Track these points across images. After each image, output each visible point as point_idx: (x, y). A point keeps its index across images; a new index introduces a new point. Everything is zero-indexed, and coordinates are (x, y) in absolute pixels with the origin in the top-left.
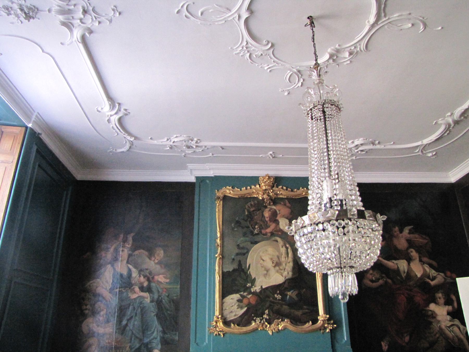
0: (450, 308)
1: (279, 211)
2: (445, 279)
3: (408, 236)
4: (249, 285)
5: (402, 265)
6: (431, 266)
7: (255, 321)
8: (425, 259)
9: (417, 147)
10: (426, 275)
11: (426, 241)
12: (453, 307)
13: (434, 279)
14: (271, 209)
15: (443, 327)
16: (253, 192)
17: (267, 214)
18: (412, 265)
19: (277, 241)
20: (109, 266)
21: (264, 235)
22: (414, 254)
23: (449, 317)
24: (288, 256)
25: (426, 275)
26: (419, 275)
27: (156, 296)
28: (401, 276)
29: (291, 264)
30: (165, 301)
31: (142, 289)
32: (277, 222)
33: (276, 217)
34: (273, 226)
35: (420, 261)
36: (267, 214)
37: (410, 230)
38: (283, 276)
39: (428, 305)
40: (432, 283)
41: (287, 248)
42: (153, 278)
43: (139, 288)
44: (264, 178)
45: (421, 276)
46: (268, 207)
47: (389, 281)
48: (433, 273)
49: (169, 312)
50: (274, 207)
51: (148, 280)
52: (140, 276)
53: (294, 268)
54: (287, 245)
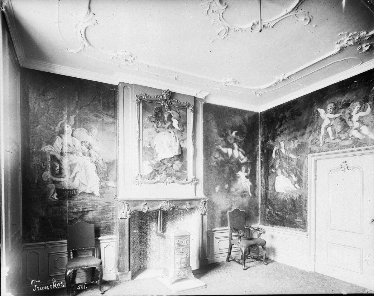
0: (246, 174)
1: (173, 114)
2: (247, 160)
3: (235, 136)
4: (154, 157)
5: (230, 151)
6: (242, 153)
7: (157, 176)
8: (241, 150)
9: (252, 90)
10: (239, 157)
11: (242, 140)
12: (248, 174)
13: (243, 159)
14: (168, 113)
15: (242, 183)
16: (158, 100)
17: (166, 116)
18: (234, 151)
19: (170, 132)
20: (59, 137)
21: (163, 128)
22: (236, 146)
23: (245, 178)
24: (176, 142)
25: (239, 157)
26: (236, 157)
27: (94, 160)
28: (228, 157)
29: (177, 147)
30: (101, 163)
31: (84, 154)
32: (171, 121)
33: (171, 118)
34: (169, 123)
35: (238, 150)
36: (166, 116)
37: (236, 133)
38: (172, 153)
39: (238, 172)
40: (242, 162)
41: (176, 138)
42: (92, 147)
43: (82, 153)
44: (166, 92)
45: (238, 158)
46: (167, 111)
47: (223, 158)
48: (242, 156)
49: (103, 169)
50: (170, 112)
51: (88, 148)
52: (82, 145)
53: (179, 149)
54: (176, 136)
